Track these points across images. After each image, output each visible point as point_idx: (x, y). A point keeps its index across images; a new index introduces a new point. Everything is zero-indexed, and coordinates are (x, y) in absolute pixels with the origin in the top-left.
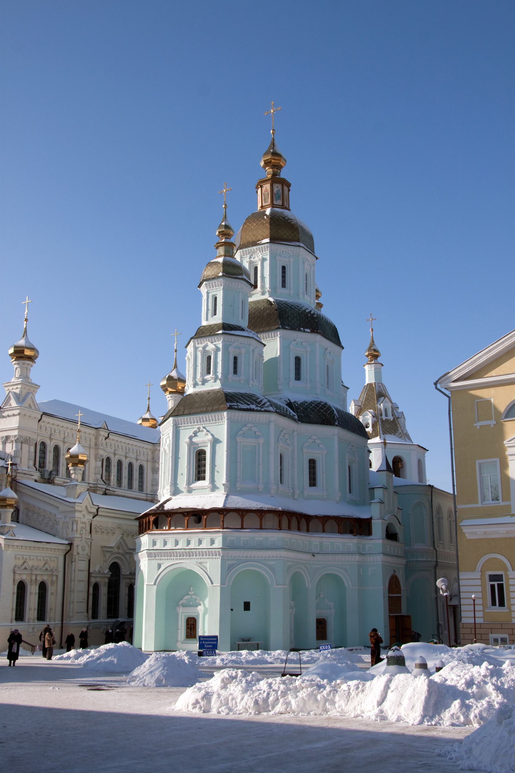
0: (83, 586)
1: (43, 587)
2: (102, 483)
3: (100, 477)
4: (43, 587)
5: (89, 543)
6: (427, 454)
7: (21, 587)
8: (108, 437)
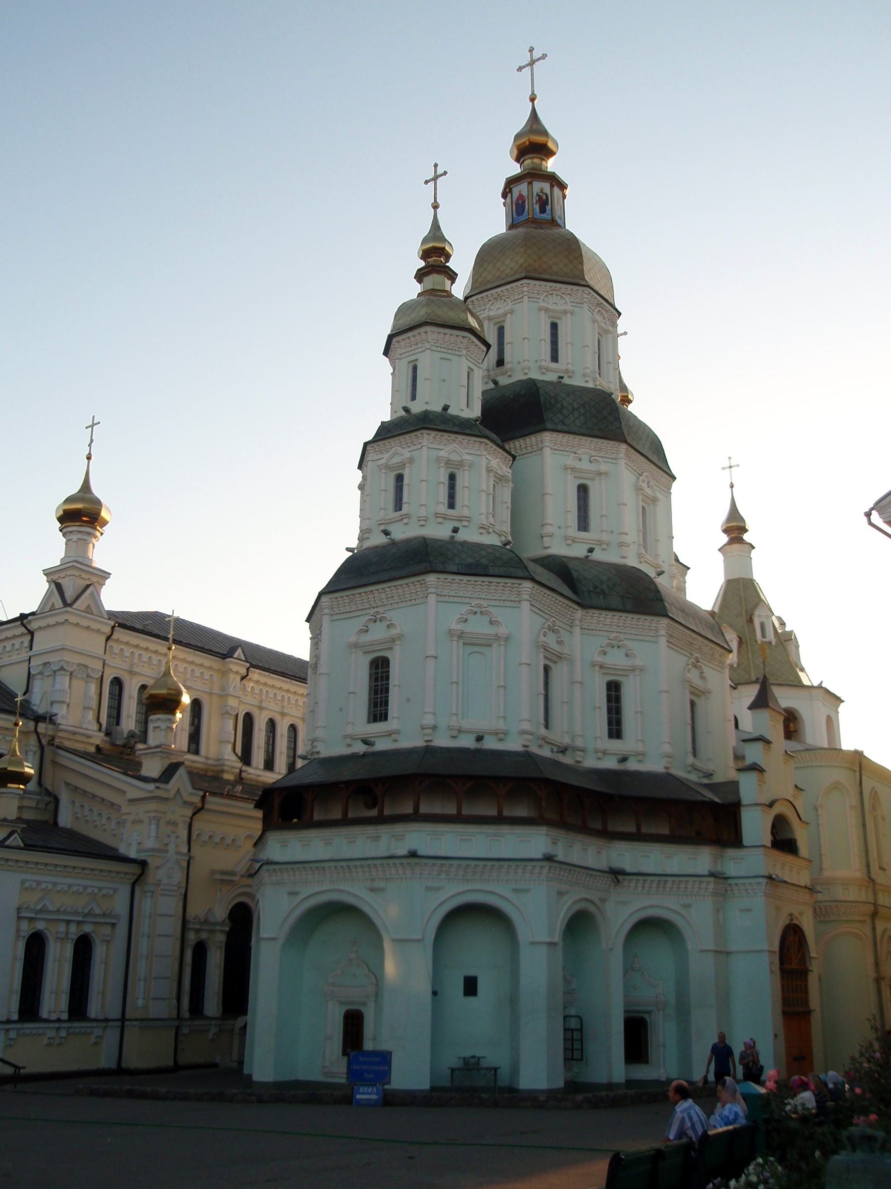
0: (169, 947)
1: (83, 948)
2: (234, 758)
3: (230, 747)
4: (83, 948)
5: (185, 864)
6: (842, 708)
7: (35, 946)
8: (247, 675)
